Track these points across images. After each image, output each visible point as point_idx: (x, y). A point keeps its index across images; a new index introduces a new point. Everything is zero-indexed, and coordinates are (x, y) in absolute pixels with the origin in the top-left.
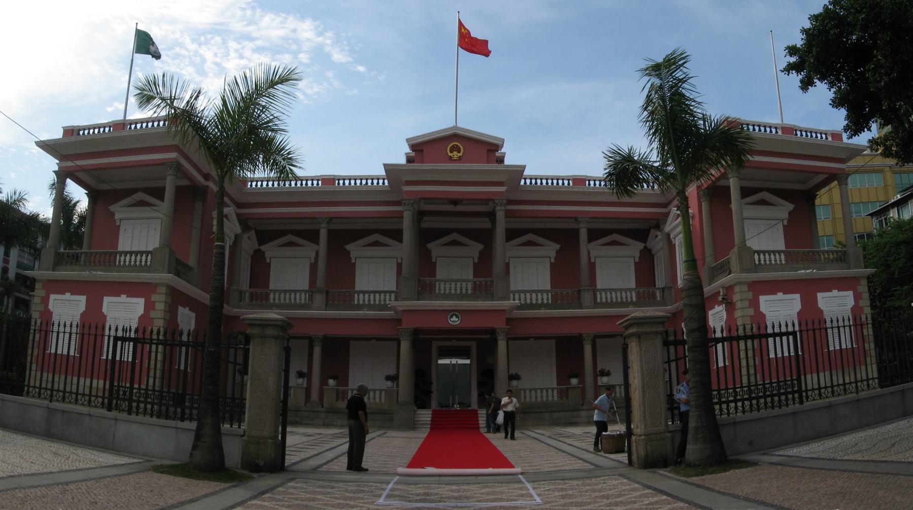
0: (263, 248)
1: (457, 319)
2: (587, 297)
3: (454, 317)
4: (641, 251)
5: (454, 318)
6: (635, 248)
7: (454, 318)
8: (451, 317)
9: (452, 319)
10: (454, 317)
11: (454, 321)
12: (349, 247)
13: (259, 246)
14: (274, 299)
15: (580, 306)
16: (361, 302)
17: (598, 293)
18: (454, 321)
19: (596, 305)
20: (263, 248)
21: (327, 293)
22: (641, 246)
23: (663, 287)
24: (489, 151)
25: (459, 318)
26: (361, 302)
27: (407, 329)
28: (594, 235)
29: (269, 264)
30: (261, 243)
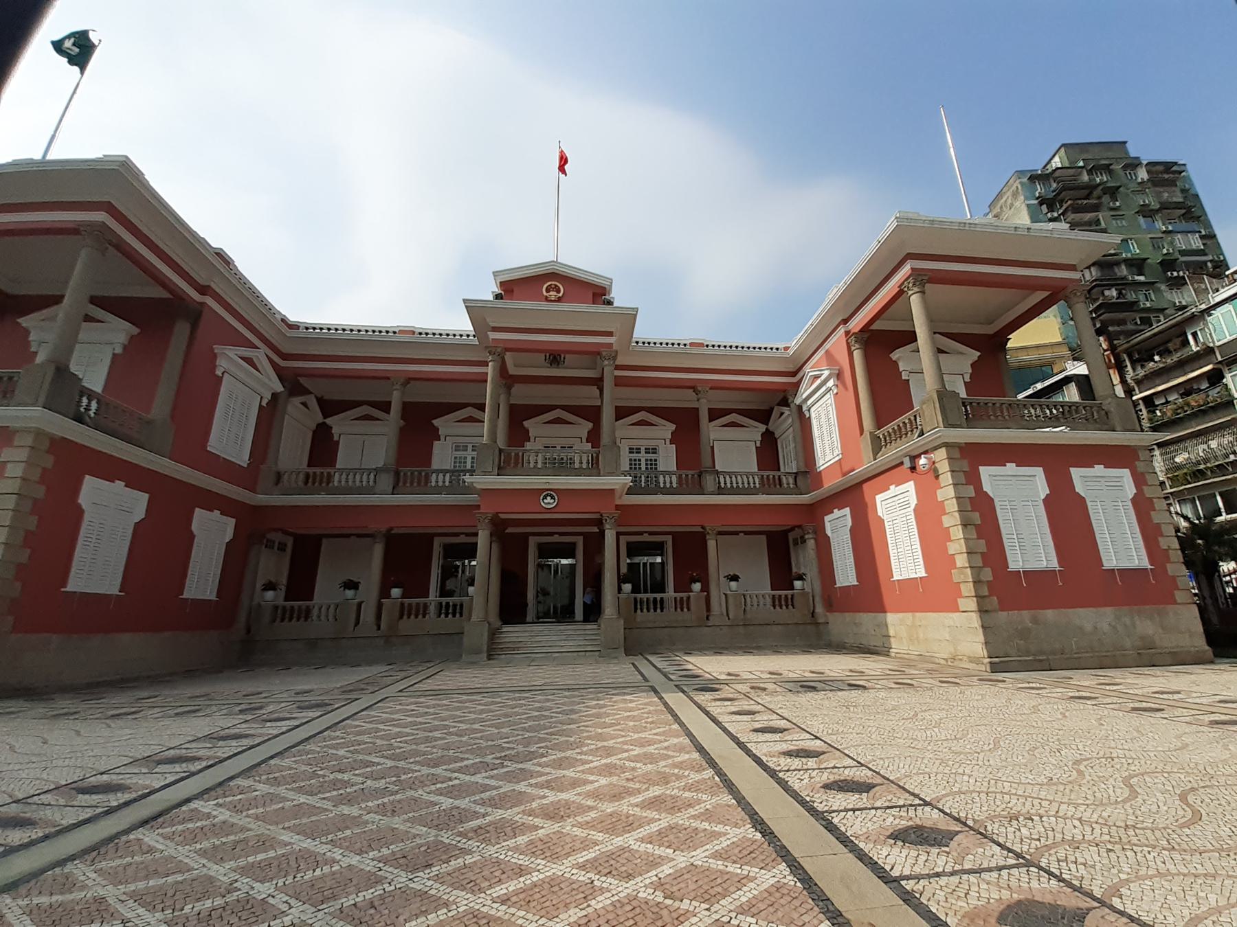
0: (329, 421)
1: (553, 501)
2: (709, 481)
3: (549, 498)
4: (762, 435)
5: (549, 500)
6: (755, 431)
7: (549, 500)
8: (545, 498)
9: (545, 501)
10: (549, 498)
11: (549, 503)
12: (436, 422)
13: (325, 418)
14: (340, 481)
15: (701, 492)
16: (440, 484)
17: (721, 477)
18: (549, 503)
19: (721, 491)
20: (329, 421)
21: (397, 474)
22: (762, 428)
23: (795, 471)
24: (594, 295)
25: (554, 499)
26: (440, 484)
27: (487, 513)
28: (714, 414)
29: (338, 442)
30: (325, 418)
